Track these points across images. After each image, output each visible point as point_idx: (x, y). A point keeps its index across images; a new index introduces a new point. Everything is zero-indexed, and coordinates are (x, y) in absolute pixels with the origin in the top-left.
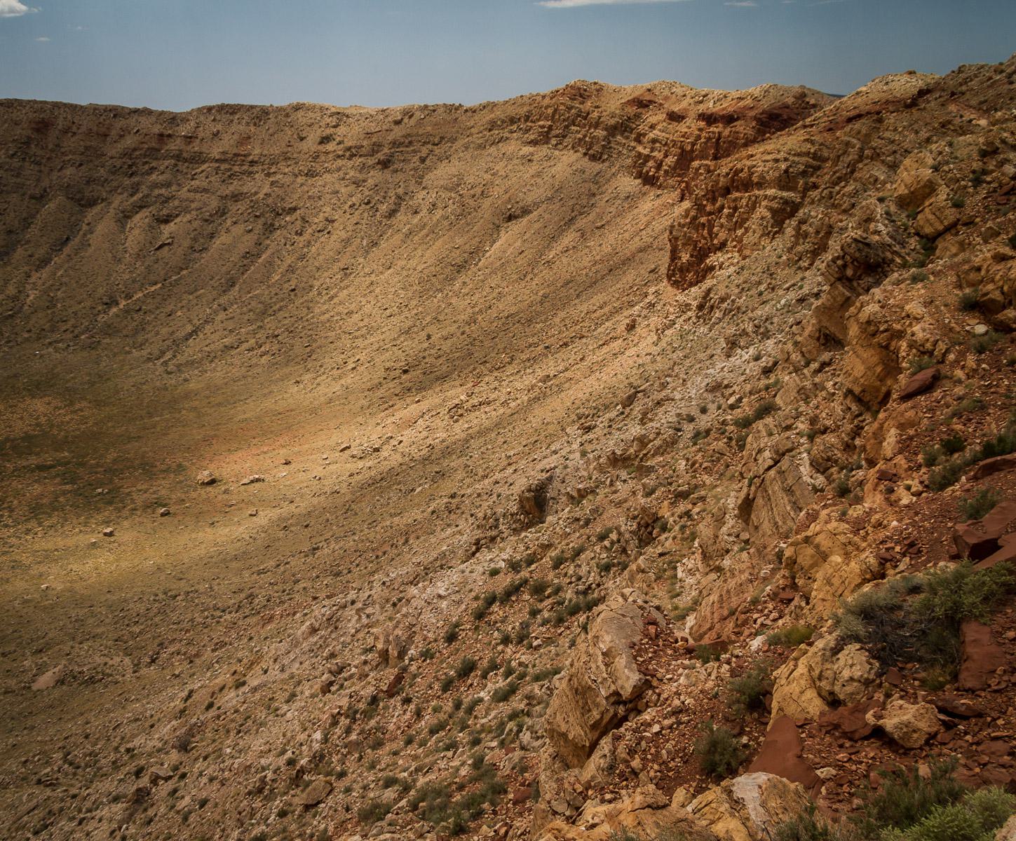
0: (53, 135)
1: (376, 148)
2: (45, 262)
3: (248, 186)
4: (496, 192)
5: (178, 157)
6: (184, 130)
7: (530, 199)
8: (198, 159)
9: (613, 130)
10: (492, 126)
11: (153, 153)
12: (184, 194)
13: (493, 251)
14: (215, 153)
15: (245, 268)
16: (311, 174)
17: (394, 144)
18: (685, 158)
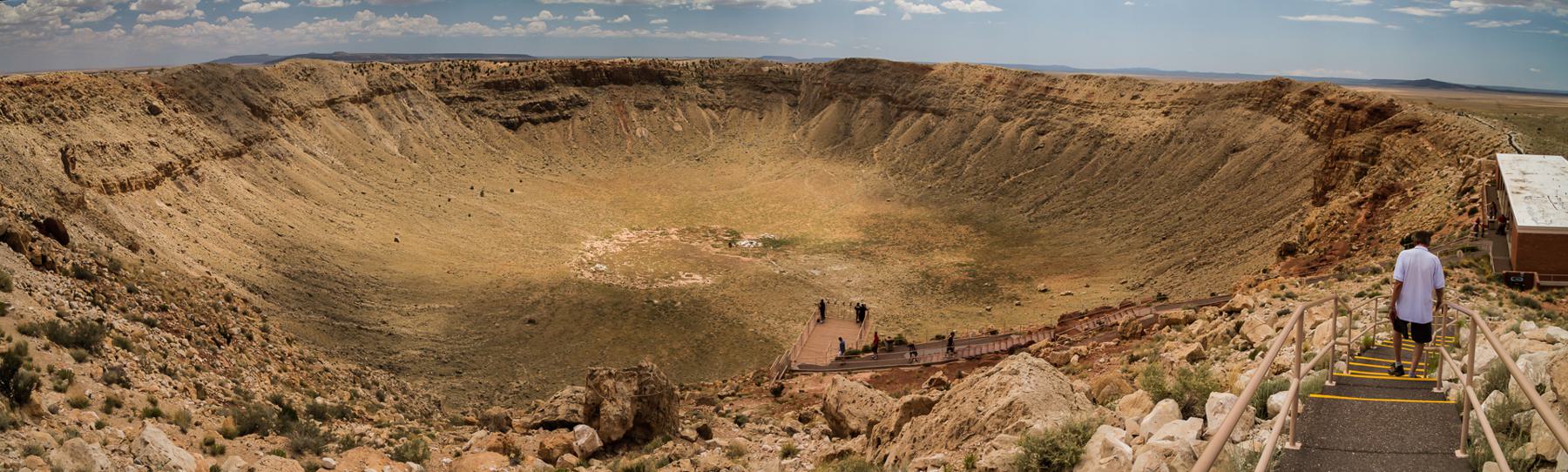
0: (993, 83)
1: (1163, 104)
2: (977, 149)
3: (1089, 120)
4: (1227, 135)
5: (1054, 100)
6: (1059, 86)
7: (1247, 140)
8: (1064, 102)
9: (1295, 107)
10: (1229, 97)
11: (1041, 97)
12: (1054, 120)
13: (1222, 170)
14: (1074, 100)
15: (1081, 166)
16: (1124, 116)
17: (1173, 103)
18: (1332, 126)
